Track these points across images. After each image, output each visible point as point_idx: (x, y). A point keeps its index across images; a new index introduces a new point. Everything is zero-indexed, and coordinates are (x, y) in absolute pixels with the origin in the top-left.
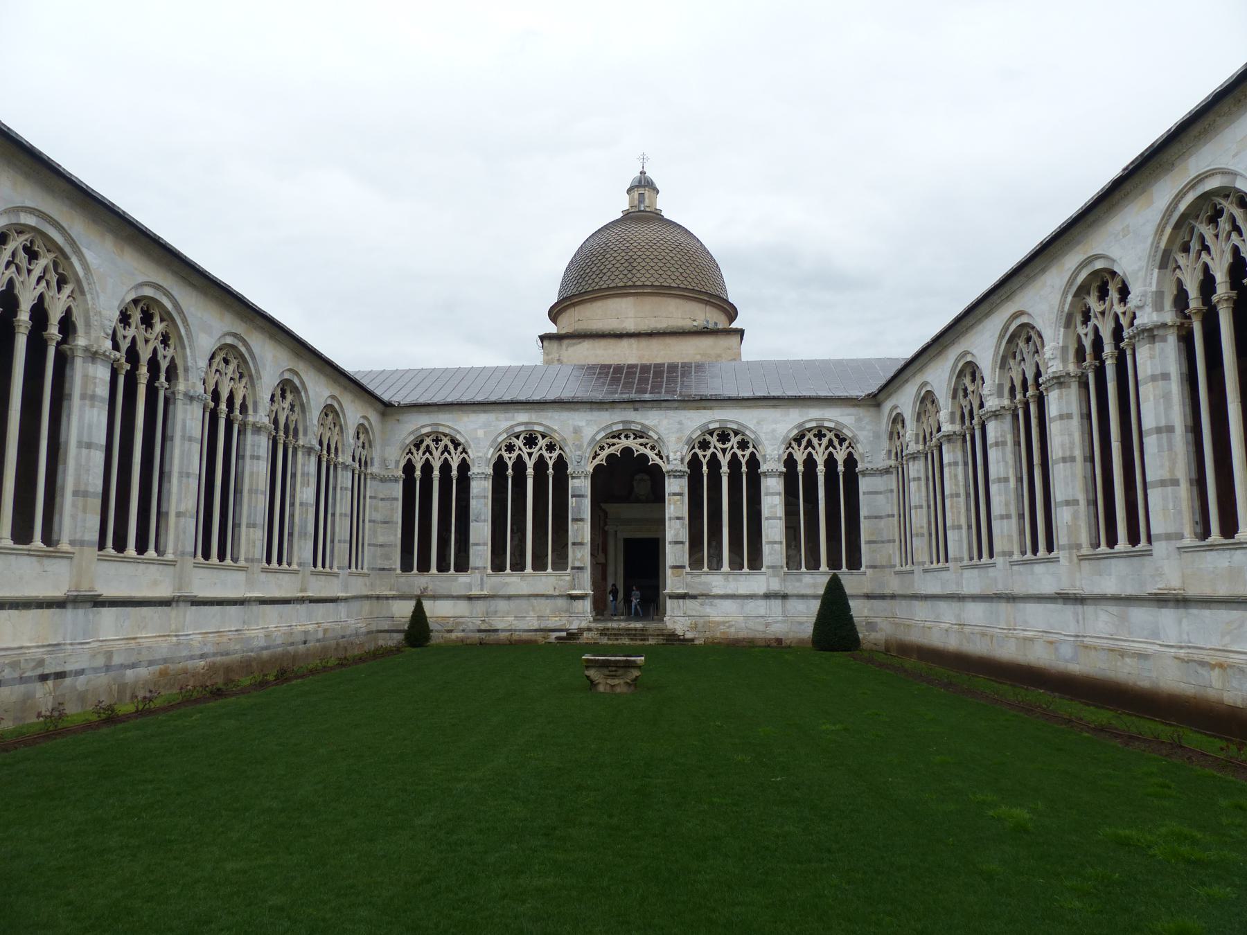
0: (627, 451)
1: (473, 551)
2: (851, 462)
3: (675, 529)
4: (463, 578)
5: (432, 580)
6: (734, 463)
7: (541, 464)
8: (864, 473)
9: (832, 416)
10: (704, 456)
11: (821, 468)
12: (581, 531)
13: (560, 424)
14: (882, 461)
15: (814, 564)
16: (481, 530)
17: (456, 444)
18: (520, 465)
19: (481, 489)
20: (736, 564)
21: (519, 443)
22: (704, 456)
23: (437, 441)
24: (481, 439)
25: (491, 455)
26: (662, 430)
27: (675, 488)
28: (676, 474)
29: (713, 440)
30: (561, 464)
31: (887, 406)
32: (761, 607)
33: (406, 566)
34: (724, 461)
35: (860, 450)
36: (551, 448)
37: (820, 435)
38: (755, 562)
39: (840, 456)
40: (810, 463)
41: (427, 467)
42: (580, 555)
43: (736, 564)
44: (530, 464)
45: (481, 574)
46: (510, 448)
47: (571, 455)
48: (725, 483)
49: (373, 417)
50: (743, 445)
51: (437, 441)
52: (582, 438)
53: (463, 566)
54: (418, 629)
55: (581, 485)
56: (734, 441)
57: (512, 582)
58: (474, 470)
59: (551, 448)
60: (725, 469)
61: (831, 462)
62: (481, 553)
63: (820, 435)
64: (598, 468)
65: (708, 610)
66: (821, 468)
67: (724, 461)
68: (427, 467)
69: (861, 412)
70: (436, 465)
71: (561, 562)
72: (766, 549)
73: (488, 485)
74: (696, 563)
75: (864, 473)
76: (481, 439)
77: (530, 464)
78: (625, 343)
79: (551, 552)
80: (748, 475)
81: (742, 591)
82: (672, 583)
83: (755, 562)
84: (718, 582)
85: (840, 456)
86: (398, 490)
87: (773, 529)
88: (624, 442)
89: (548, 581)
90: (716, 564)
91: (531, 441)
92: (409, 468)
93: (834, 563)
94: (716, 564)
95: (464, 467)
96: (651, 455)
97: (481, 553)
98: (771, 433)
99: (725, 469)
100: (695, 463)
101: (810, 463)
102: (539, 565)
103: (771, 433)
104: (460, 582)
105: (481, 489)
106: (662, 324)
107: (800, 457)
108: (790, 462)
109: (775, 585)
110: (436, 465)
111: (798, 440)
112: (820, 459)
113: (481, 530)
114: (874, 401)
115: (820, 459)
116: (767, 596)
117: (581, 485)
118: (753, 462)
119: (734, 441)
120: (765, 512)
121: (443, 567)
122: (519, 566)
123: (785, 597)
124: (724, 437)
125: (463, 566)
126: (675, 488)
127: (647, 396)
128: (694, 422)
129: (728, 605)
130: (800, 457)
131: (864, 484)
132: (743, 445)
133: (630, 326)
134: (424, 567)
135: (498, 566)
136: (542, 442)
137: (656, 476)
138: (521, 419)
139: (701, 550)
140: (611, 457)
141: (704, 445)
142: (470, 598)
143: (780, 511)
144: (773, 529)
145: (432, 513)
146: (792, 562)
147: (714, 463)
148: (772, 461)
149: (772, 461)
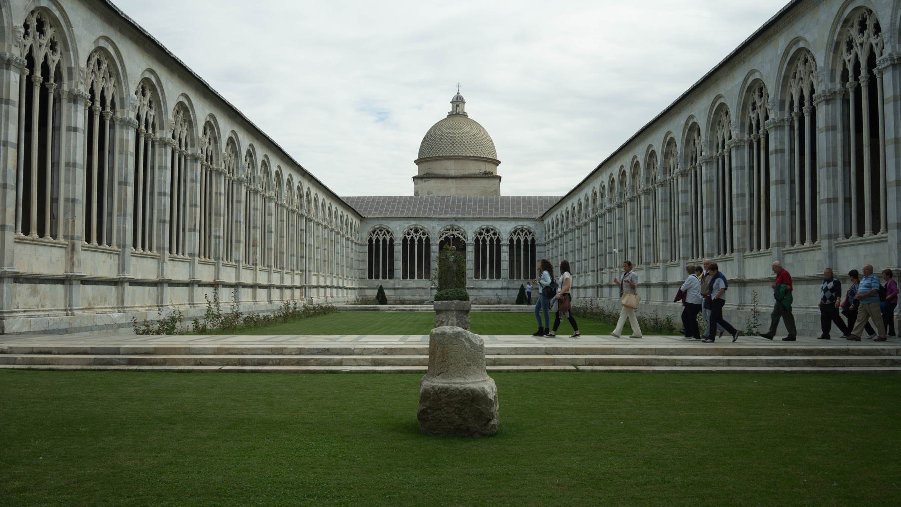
0: (452, 235)
1: (396, 272)
2: (533, 241)
3: (470, 265)
4: (392, 281)
5: (380, 282)
6: (491, 240)
7: (420, 240)
8: (538, 245)
9: (526, 224)
10: (480, 238)
11: (522, 243)
12: (435, 265)
13: (427, 225)
14: (543, 242)
15: (519, 277)
16: (399, 264)
17: (389, 232)
18: (413, 240)
19: (398, 249)
20: (491, 277)
21: (412, 232)
22: (480, 238)
23: (381, 230)
24: (399, 230)
25: (402, 236)
26: (465, 228)
27: (470, 250)
28: (469, 244)
29: (484, 232)
30: (428, 240)
31: (546, 222)
32: (499, 292)
33: (371, 277)
34: (488, 240)
35: (536, 236)
36: (424, 234)
37: (522, 231)
38: (498, 277)
39: (529, 239)
40: (518, 241)
41: (378, 241)
42: (435, 273)
43: (491, 277)
44: (416, 240)
45: (398, 280)
46: (409, 234)
47: (431, 236)
48: (487, 247)
49: (358, 222)
50: (494, 234)
51: (381, 230)
52: (436, 230)
53: (392, 276)
54: (382, 298)
55: (435, 248)
56: (491, 232)
57: (411, 283)
58: (396, 242)
59: (424, 234)
60: (488, 243)
61: (526, 241)
62: (399, 272)
63: (522, 231)
64: (441, 242)
65: (481, 293)
66: (522, 243)
67: (488, 240)
68: (378, 241)
69: (537, 223)
70: (381, 240)
71: (428, 276)
72: (502, 272)
73: (401, 247)
74: (476, 277)
75: (538, 245)
76: (399, 230)
77: (416, 240)
78: (450, 181)
79: (426, 272)
80: (496, 244)
81: (493, 287)
82: (469, 284)
83: (498, 277)
84: (484, 284)
85: (529, 239)
86: (367, 248)
87: (505, 265)
88: (451, 232)
89: (424, 283)
90: (484, 277)
91: (417, 231)
92: (371, 241)
93: (526, 277)
94: (484, 277)
95: (392, 240)
96: (461, 237)
97: (399, 272)
98: (505, 229)
99: (488, 243)
100: (477, 240)
101: (518, 241)
102: (420, 277)
103: (505, 229)
104: (388, 283)
105: (398, 249)
106: (466, 172)
107: (515, 239)
108: (511, 240)
109: (505, 285)
110: (381, 240)
111: (514, 232)
112: (522, 240)
113: (399, 264)
114: (542, 218)
115: (522, 240)
116: (501, 289)
117: (435, 248)
118: (498, 240)
119: (491, 232)
120: (502, 259)
121: (384, 277)
122: (412, 277)
123: (508, 289)
124: (488, 231)
125: (392, 276)
126: (470, 250)
127: (460, 216)
128: (476, 226)
129: (488, 291)
130: (515, 239)
131: (537, 249)
132: (494, 234)
133: (452, 173)
134: (377, 277)
135: (405, 277)
136: (421, 232)
137: (461, 247)
138: (414, 223)
139: (479, 272)
140: (446, 238)
141: (480, 234)
142: (395, 289)
143: (507, 258)
144: (505, 265)
145: (378, 256)
146: (511, 276)
147: (484, 240)
148: (505, 240)
149: (505, 240)
